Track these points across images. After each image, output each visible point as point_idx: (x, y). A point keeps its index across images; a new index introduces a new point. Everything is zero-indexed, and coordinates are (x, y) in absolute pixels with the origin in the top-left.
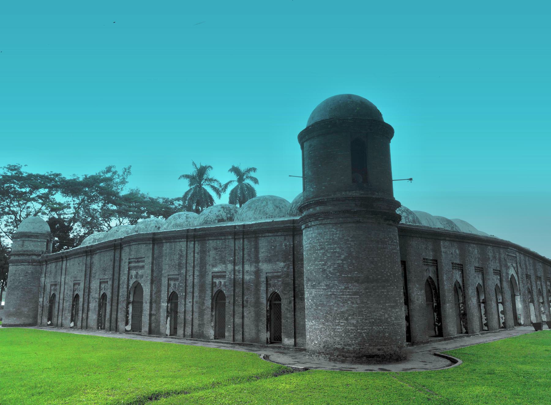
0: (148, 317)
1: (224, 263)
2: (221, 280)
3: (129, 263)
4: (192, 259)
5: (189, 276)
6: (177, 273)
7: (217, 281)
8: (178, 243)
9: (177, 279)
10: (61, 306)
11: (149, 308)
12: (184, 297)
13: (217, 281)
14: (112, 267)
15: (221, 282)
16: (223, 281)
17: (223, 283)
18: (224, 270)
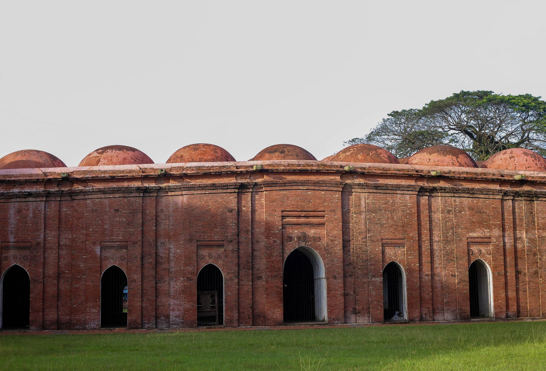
0: (342, 299)
1: (489, 227)
2: (481, 248)
3: (283, 217)
4: (427, 219)
5: (424, 241)
6: (401, 236)
7: (475, 249)
8: (399, 196)
9: (403, 245)
10: (51, 290)
11: (342, 285)
12: (417, 269)
13: (475, 249)
14: (236, 222)
15: (480, 251)
16: (483, 249)
17: (483, 251)
18: (488, 235)
